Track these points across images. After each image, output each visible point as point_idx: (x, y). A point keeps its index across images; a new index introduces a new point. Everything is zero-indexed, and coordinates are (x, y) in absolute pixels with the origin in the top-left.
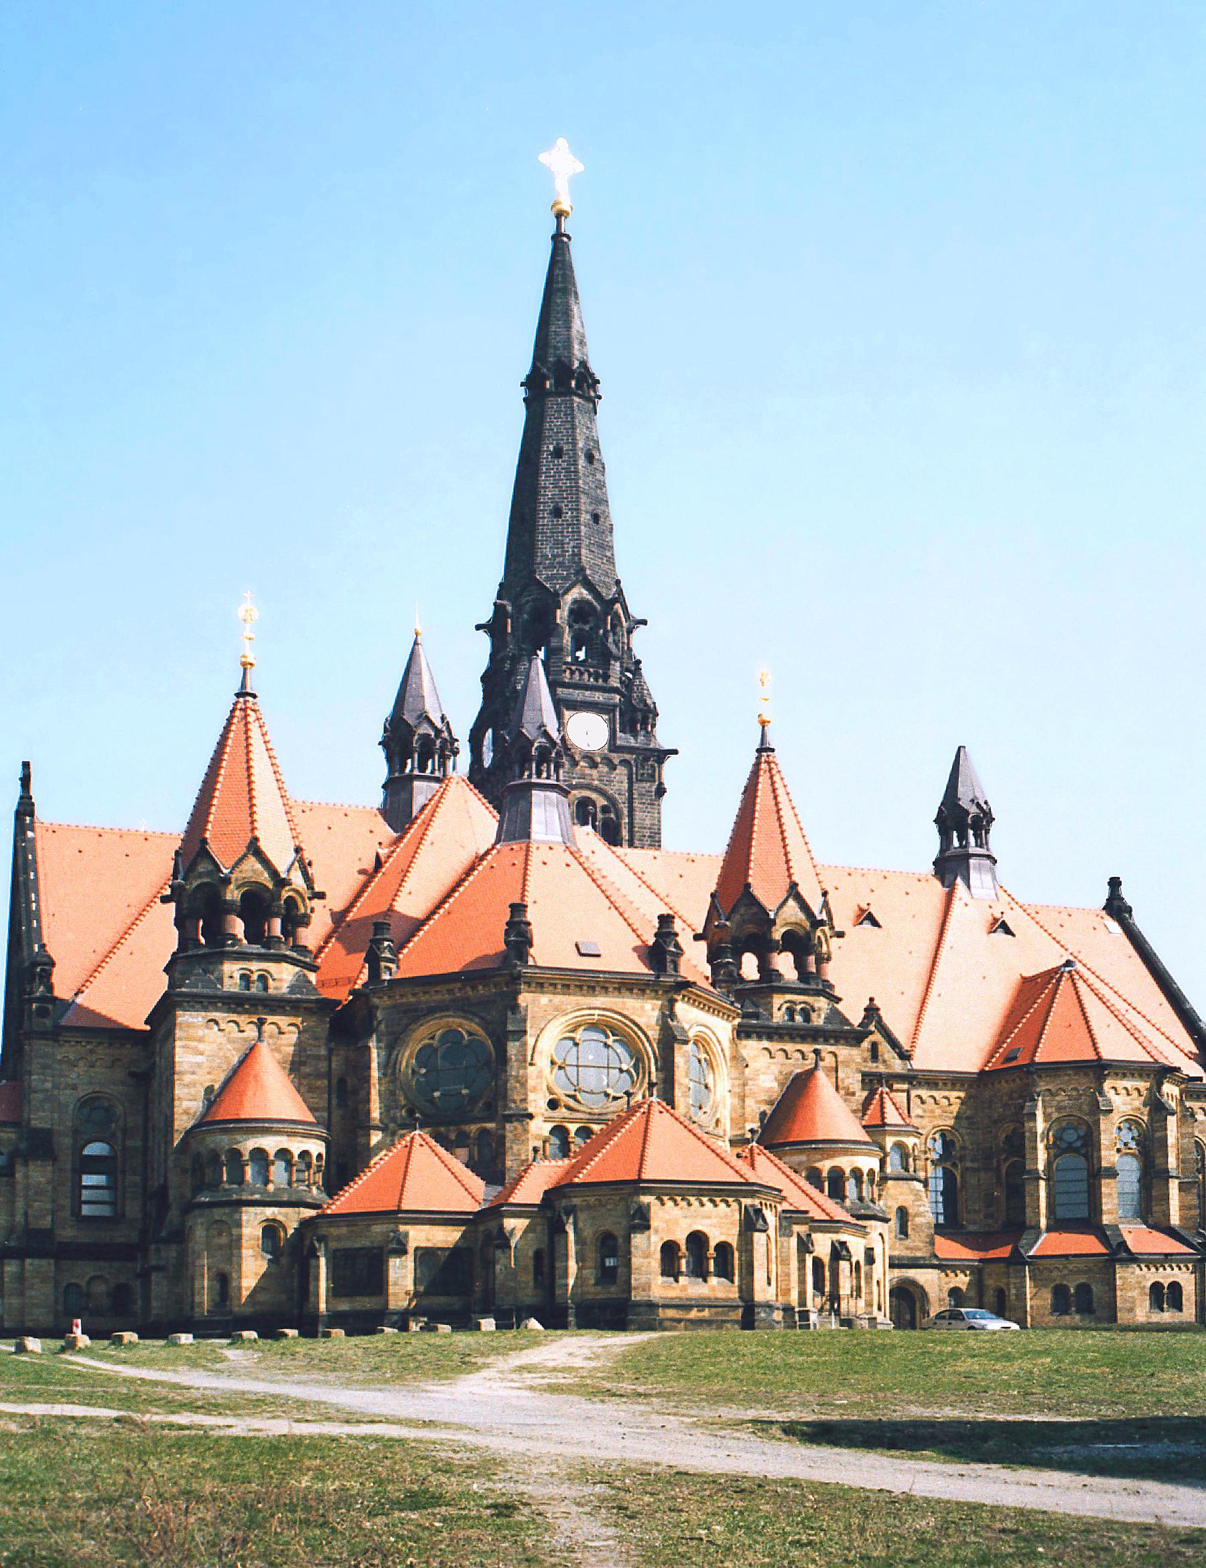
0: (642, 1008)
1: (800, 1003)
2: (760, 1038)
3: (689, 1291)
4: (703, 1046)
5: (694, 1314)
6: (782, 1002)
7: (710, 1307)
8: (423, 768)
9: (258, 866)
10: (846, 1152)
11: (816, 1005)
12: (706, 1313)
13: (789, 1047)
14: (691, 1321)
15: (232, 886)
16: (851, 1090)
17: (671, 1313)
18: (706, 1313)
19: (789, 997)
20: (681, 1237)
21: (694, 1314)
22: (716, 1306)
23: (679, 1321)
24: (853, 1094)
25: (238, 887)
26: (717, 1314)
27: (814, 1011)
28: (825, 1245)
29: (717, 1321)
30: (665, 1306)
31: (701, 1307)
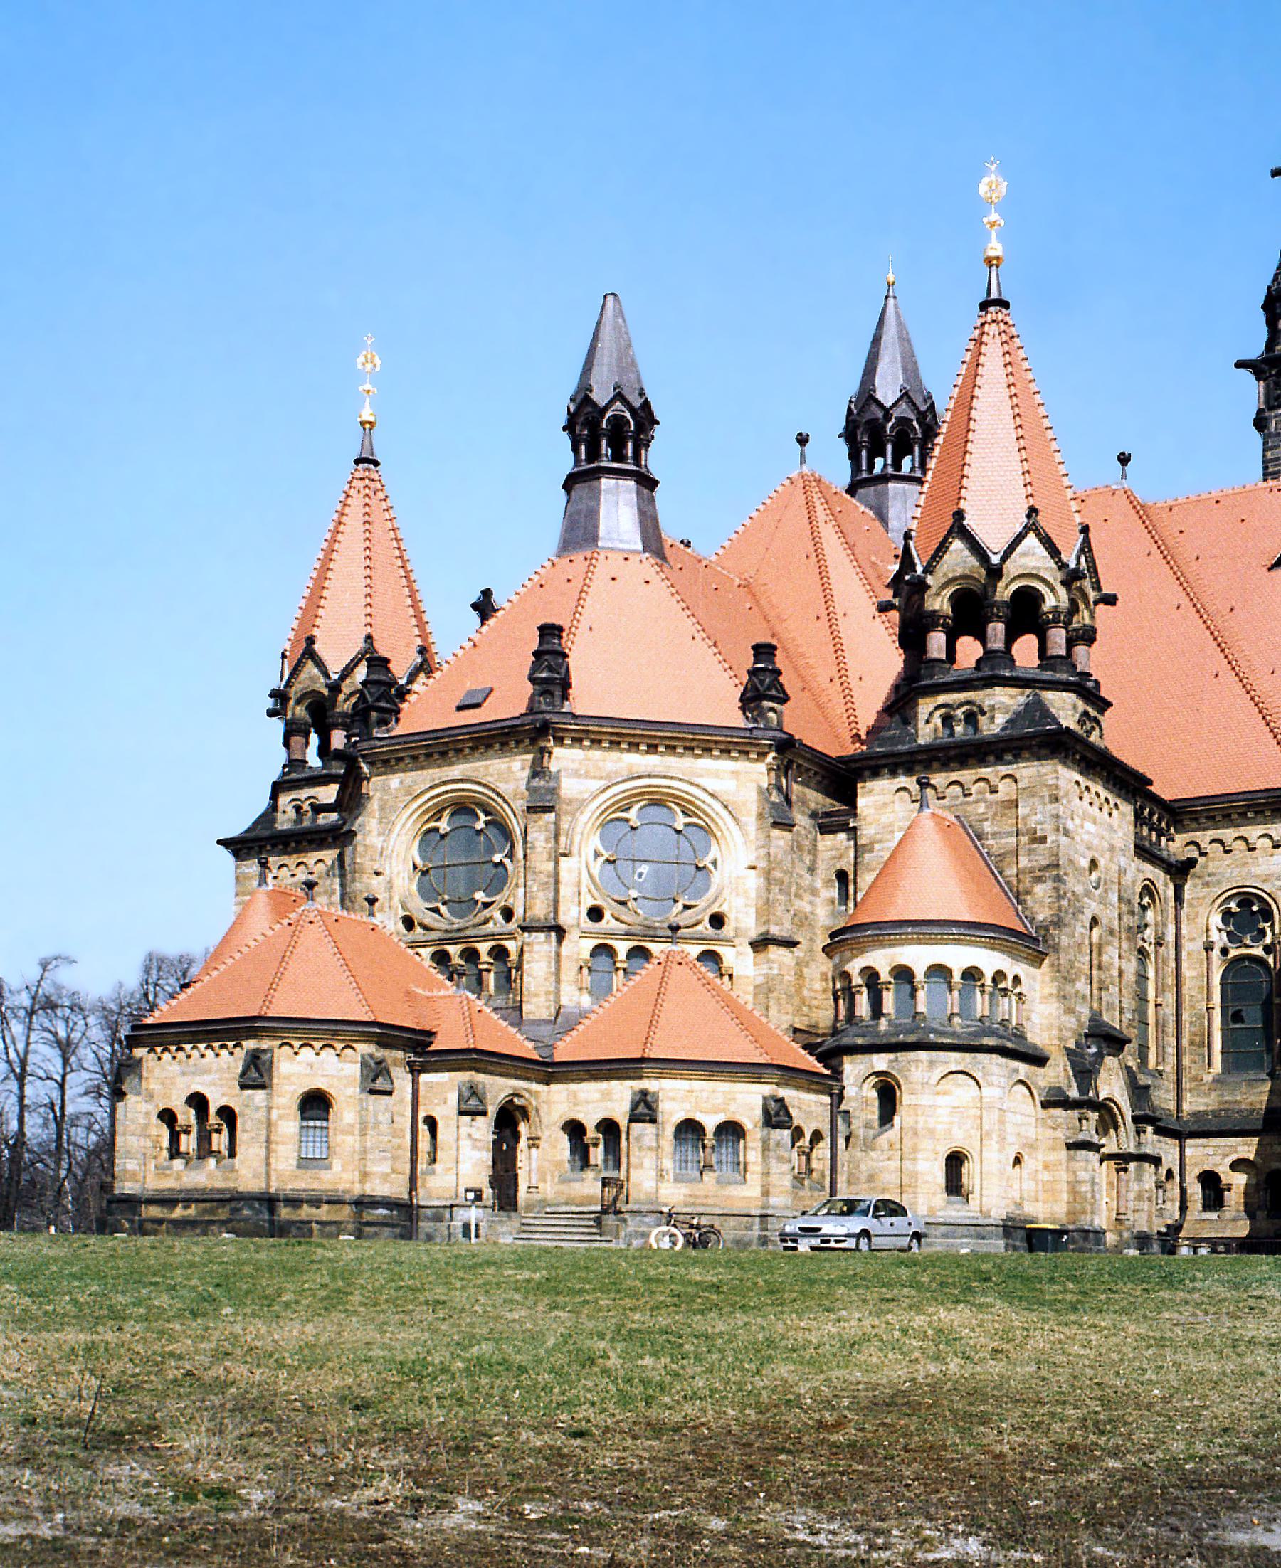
0: (509, 769)
1: (961, 705)
2: (893, 774)
3: (185, 1179)
4: (677, 804)
5: (179, 1212)
6: (931, 708)
7: (197, 1201)
8: (897, 465)
9: (316, 671)
10: (879, 942)
11: (987, 704)
12: (192, 1211)
13: (966, 776)
14: (176, 1223)
15: (292, 702)
16: (1039, 834)
17: (154, 1211)
18: (192, 1211)
19: (943, 699)
20: (177, 1103)
21: (179, 1212)
22: (204, 1201)
23: (160, 1222)
24: (1043, 840)
25: (298, 702)
26: (205, 1211)
27: (983, 713)
28: (622, 1099)
29: (201, 1222)
30: (150, 1201)
31: (187, 1202)
